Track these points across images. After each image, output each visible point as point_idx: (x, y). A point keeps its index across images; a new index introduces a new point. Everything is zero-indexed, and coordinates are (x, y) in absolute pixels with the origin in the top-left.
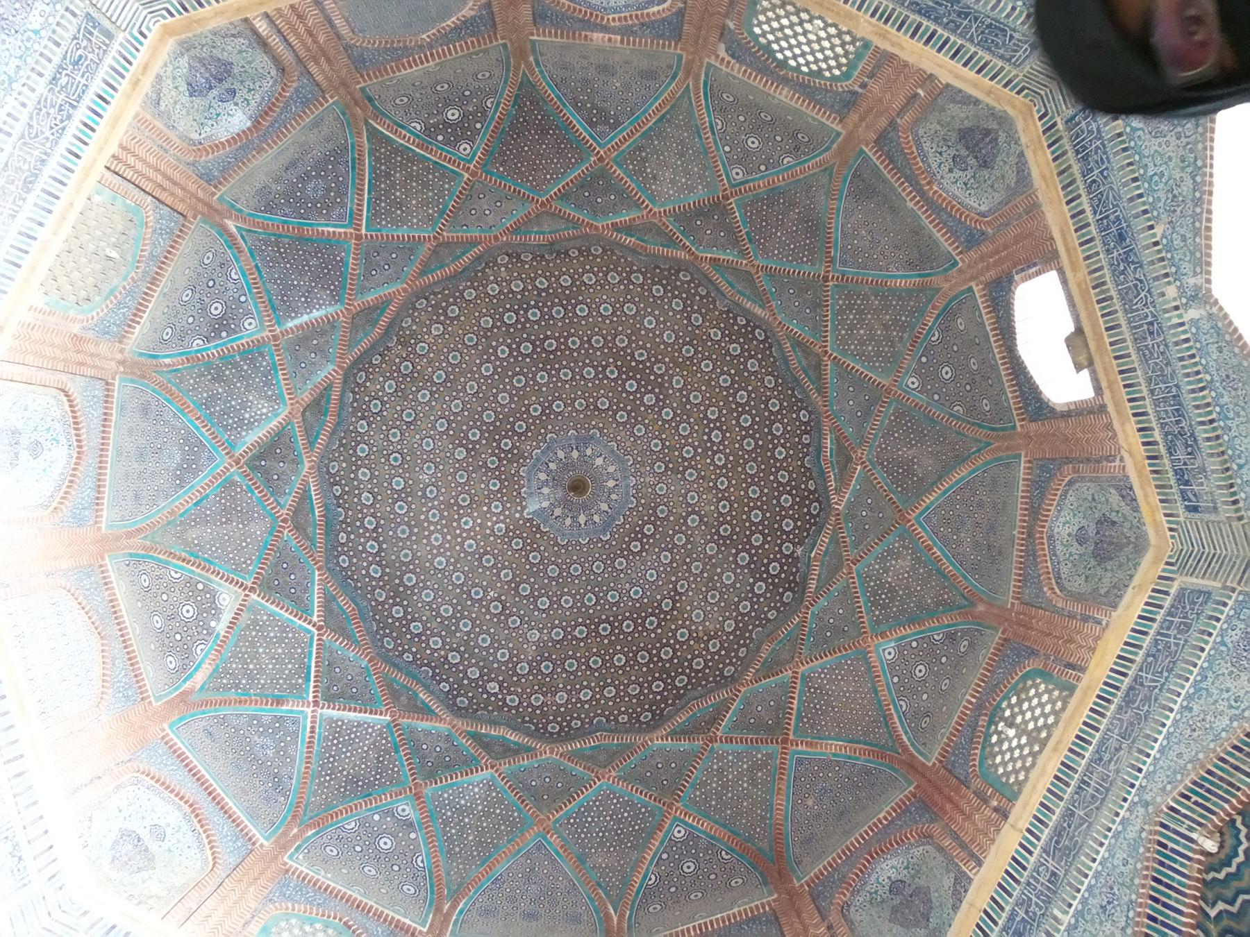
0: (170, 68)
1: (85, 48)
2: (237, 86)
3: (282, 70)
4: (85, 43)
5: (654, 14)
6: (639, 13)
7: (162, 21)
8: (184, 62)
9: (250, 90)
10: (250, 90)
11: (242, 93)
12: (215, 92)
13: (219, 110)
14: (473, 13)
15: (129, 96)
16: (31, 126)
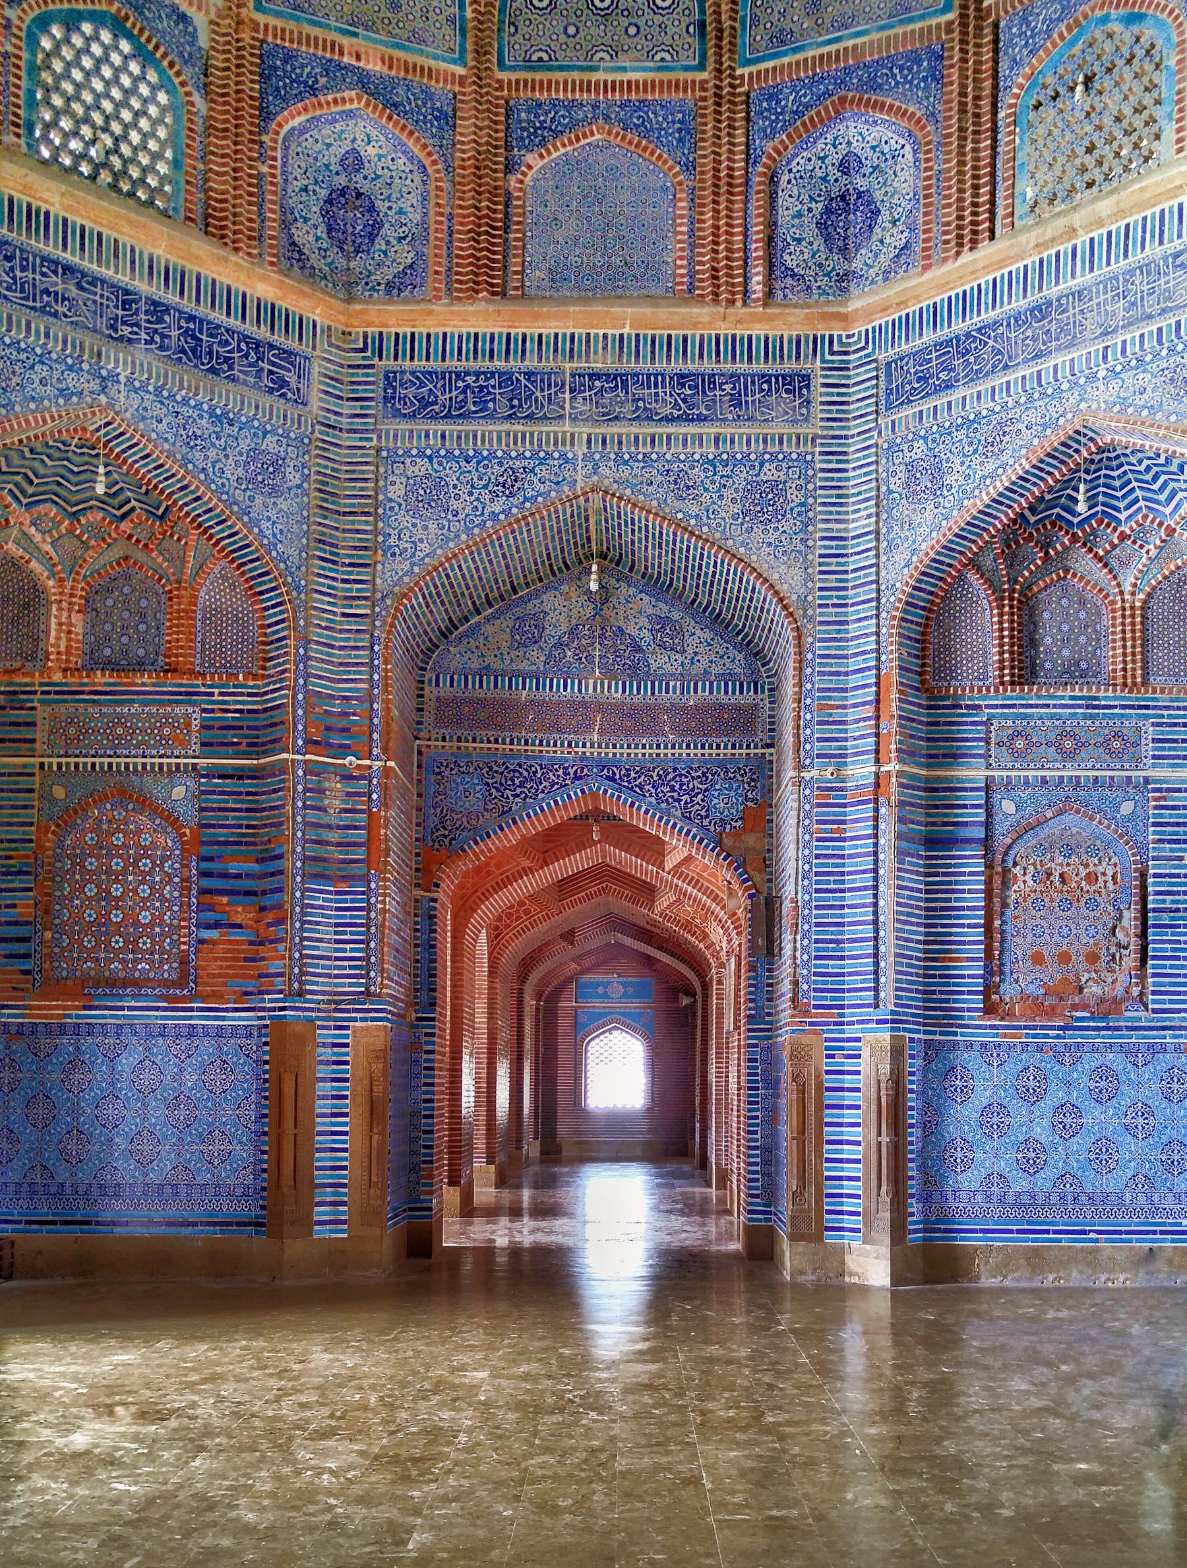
0: (872, 272)
1: (910, 383)
2: (834, 173)
3: (773, 180)
4: (908, 387)
5: (299, 113)
6: (318, 113)
7: (844, 334)
8: (857, 264)
9: (822, 159)
10: (822, 159)
11: (834, 158)
12: (860, 183)
13: (870, 153)
14: (530, 158)
15: (916, 297)
16: (994, 366)
